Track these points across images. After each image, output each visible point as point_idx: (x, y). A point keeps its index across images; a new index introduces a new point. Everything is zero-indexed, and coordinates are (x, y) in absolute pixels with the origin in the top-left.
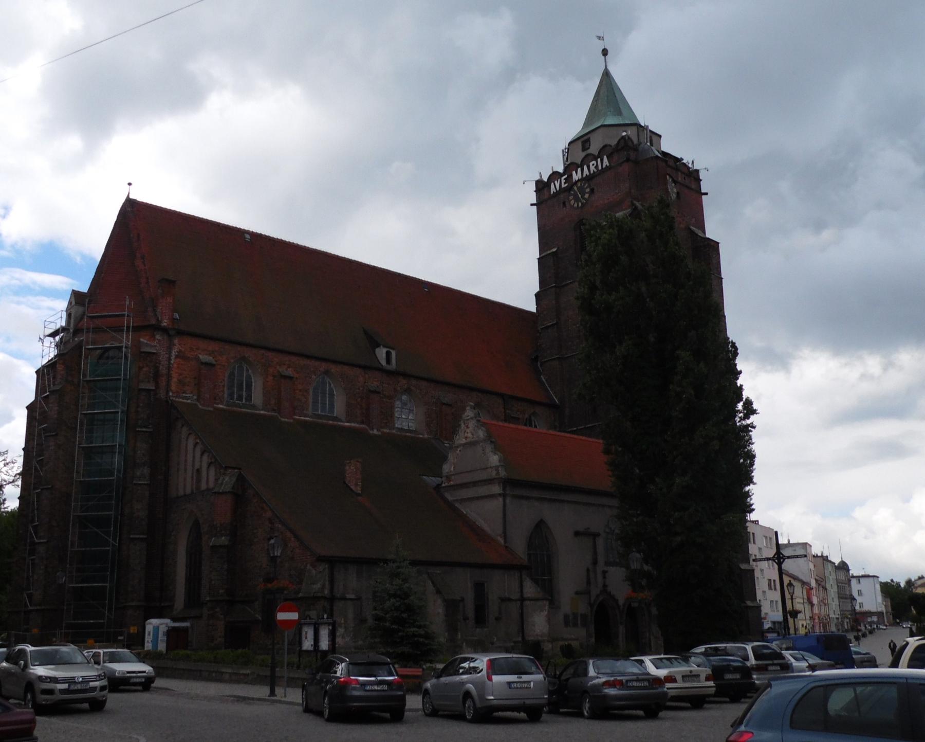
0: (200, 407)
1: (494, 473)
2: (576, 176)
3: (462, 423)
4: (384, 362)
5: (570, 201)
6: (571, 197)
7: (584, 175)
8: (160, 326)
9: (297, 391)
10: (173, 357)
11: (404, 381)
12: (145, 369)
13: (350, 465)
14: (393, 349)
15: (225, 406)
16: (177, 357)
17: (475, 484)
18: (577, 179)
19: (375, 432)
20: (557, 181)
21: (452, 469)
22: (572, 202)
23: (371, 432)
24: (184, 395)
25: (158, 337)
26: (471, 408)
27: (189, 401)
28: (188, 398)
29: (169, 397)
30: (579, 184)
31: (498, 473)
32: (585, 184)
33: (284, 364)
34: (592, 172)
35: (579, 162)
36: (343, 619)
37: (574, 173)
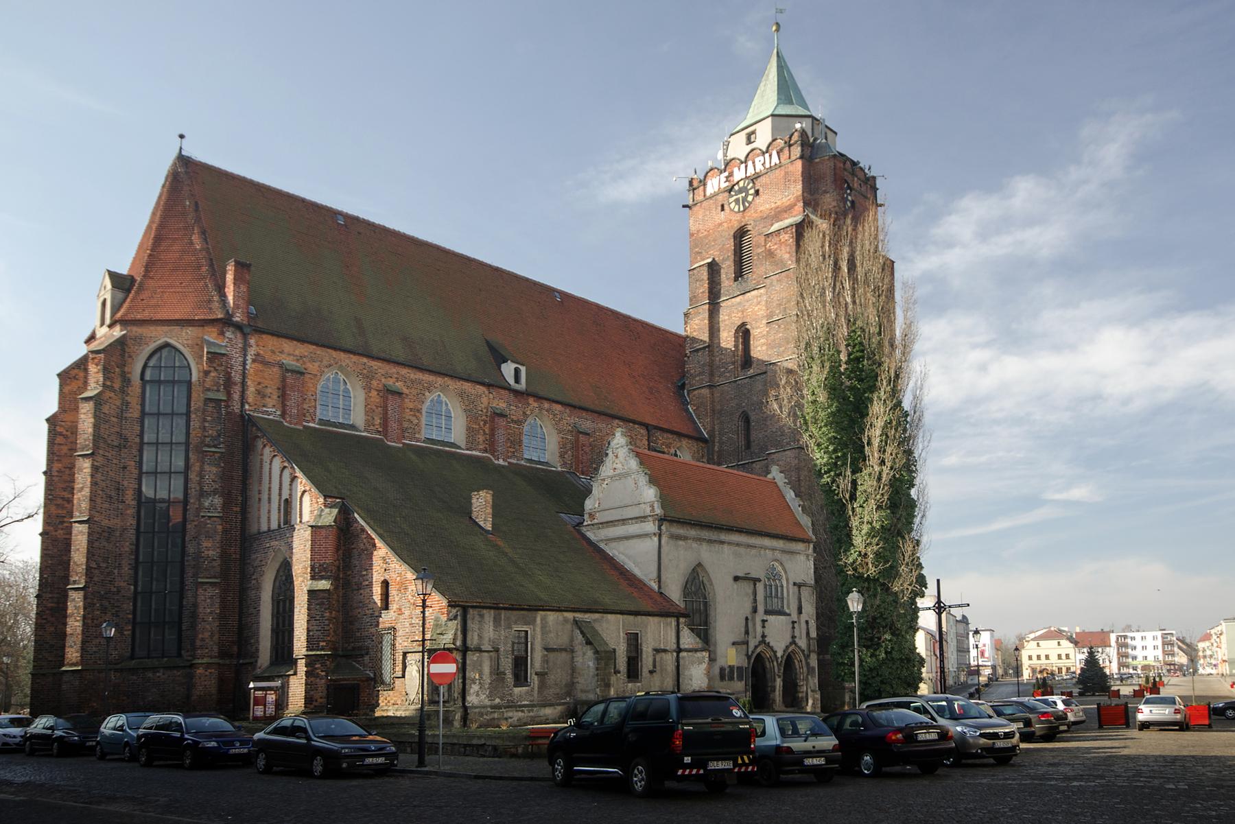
0: (286, 424)
1: (648, 510)
2: (739, 174)
3: (610, 452)
4: (511, 381)
8: (231, 320)
9: (408, 410)
10: (249, 362)
11: (536, 405)
12: (212, 374)
13: (478, 497)
14: (523, 365)
15: (317, 424)
16: (254, 361)
17: (624, 521)
19: (501, 462)
21: (597, 506)
22: (732, 205)
23: (496, 462)
24: (265, 409)
25: (228, 334)
26: (622, 434)
27: (271, 417)
28: (271, 411)
29: (245, 411)
30: (741, 184)
31: (653, 510)
32: (748, 185)
33: (391, 377)
36: (477, 675)
37: (736, 170)
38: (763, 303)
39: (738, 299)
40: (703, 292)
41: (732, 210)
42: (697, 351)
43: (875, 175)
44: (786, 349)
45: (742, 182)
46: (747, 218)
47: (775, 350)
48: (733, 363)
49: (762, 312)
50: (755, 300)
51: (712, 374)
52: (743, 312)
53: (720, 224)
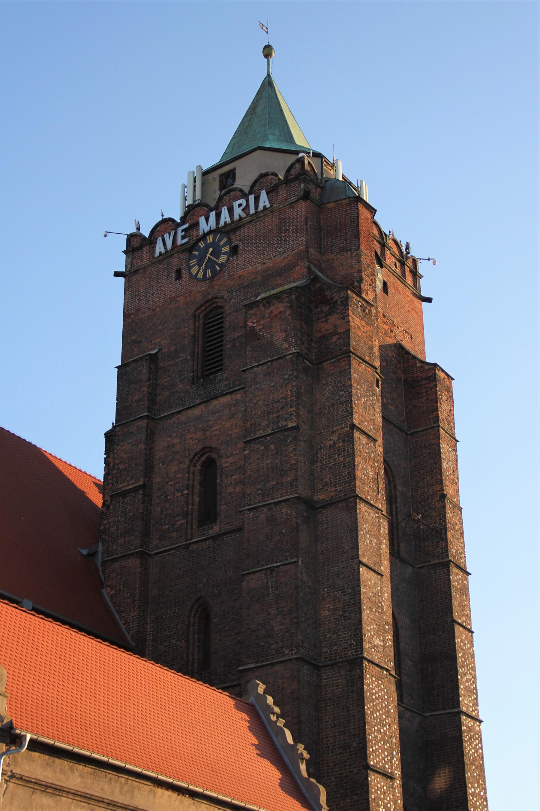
2: (204, 226)
5: (190, 268)
6: (193, 262)
7: (222, 224)
18: (207, 229)
20: (170, 233)
22: (194, 270)
30: (210, 239)
32: (220, 240)
34: (236, 217)
35: (213, 204)
37: (202, 220)
38: (240, 415)
39: (197, 412)
40: (140, 400)
41: (194, 277)
42: (124, 494)
43: (417, 257)
44: (277, 484)
45: (211, 237)
46: (217, 288)
47: (259, 487)
48: (185, 515)
49: (237, 431)
50: (227, 411)
51: (146, 534)
52: (204, 430)
53: (172, 299)
